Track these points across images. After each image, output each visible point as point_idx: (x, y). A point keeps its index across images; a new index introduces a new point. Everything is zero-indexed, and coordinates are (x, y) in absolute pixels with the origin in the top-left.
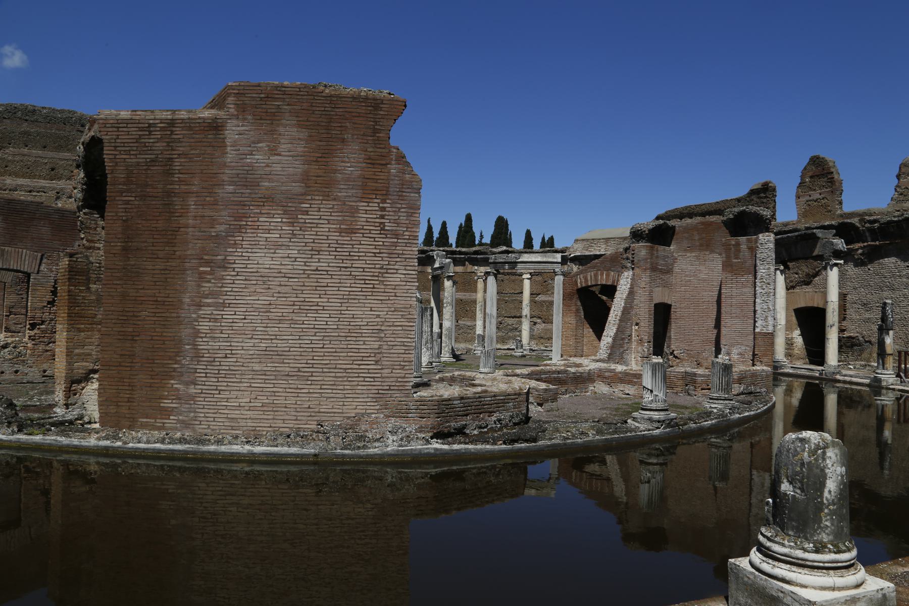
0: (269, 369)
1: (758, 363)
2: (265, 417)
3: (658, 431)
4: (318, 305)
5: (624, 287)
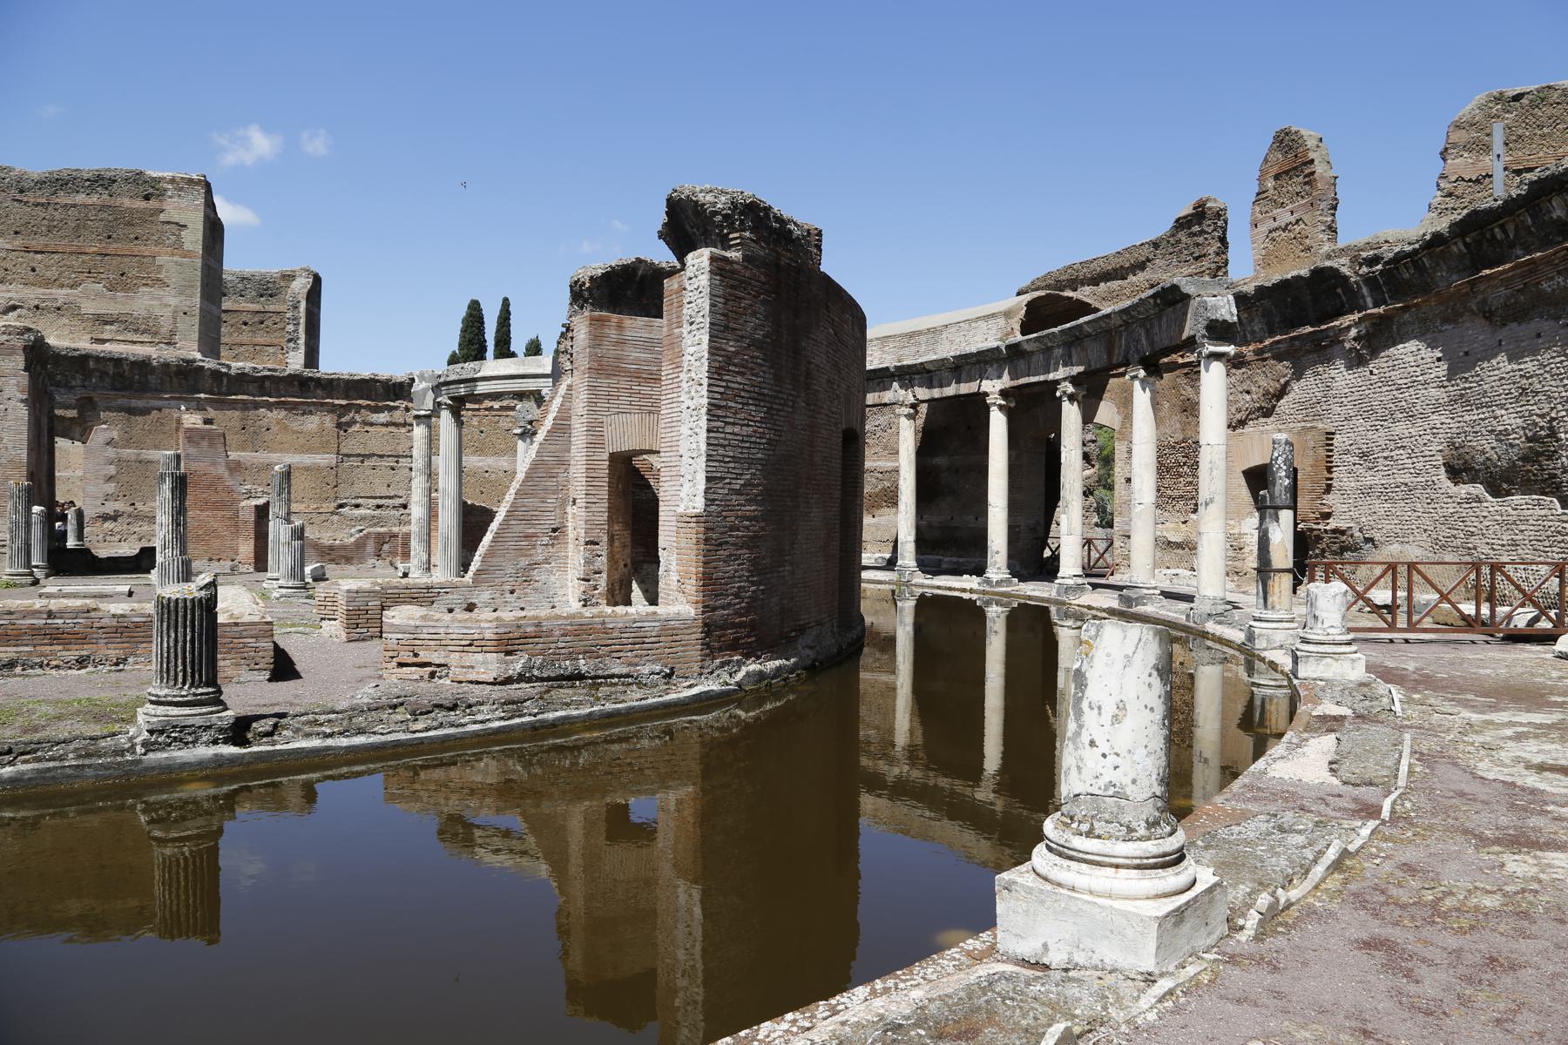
1: (680, 597)
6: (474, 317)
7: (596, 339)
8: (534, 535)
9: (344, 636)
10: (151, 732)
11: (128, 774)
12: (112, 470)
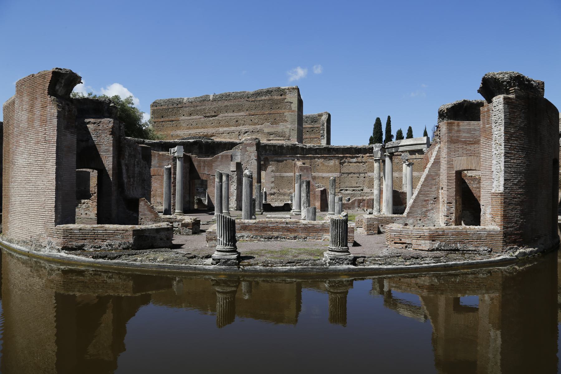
1: (493, 223)
6: (378, 123)
7: (450, 130)
8: (428, 200)
9: (366, 233)
10: (331, 259)
11: (325, 271)
12: (273, 179)
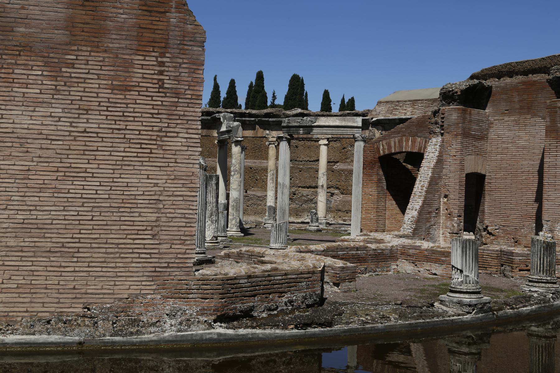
0: (27, 244)
2: (21, 300)
3: (468, 317)
4: (86, 172)
5: (431, 155)
